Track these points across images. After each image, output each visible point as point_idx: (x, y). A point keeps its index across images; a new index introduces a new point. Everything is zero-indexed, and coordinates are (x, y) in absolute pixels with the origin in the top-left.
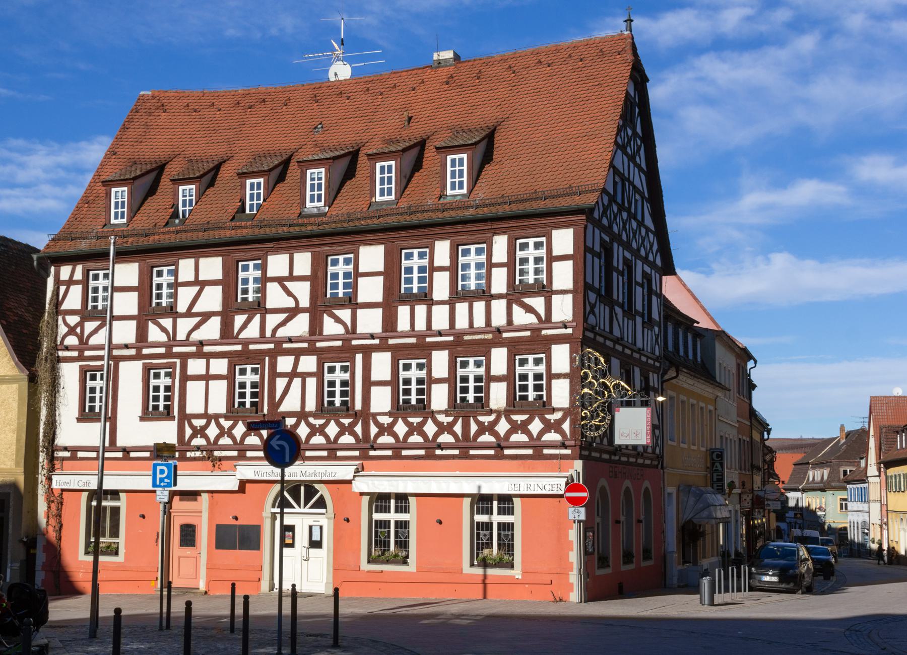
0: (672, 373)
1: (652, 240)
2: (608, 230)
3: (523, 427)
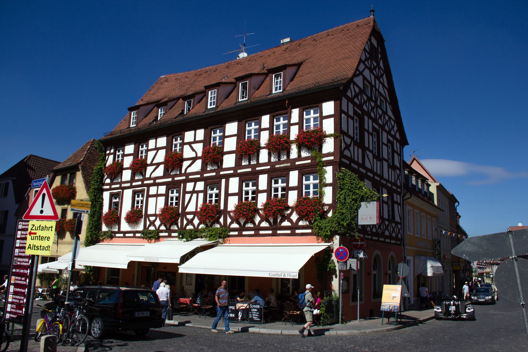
0: (408, 195)
1: (393, 124)
2: (360, 107)
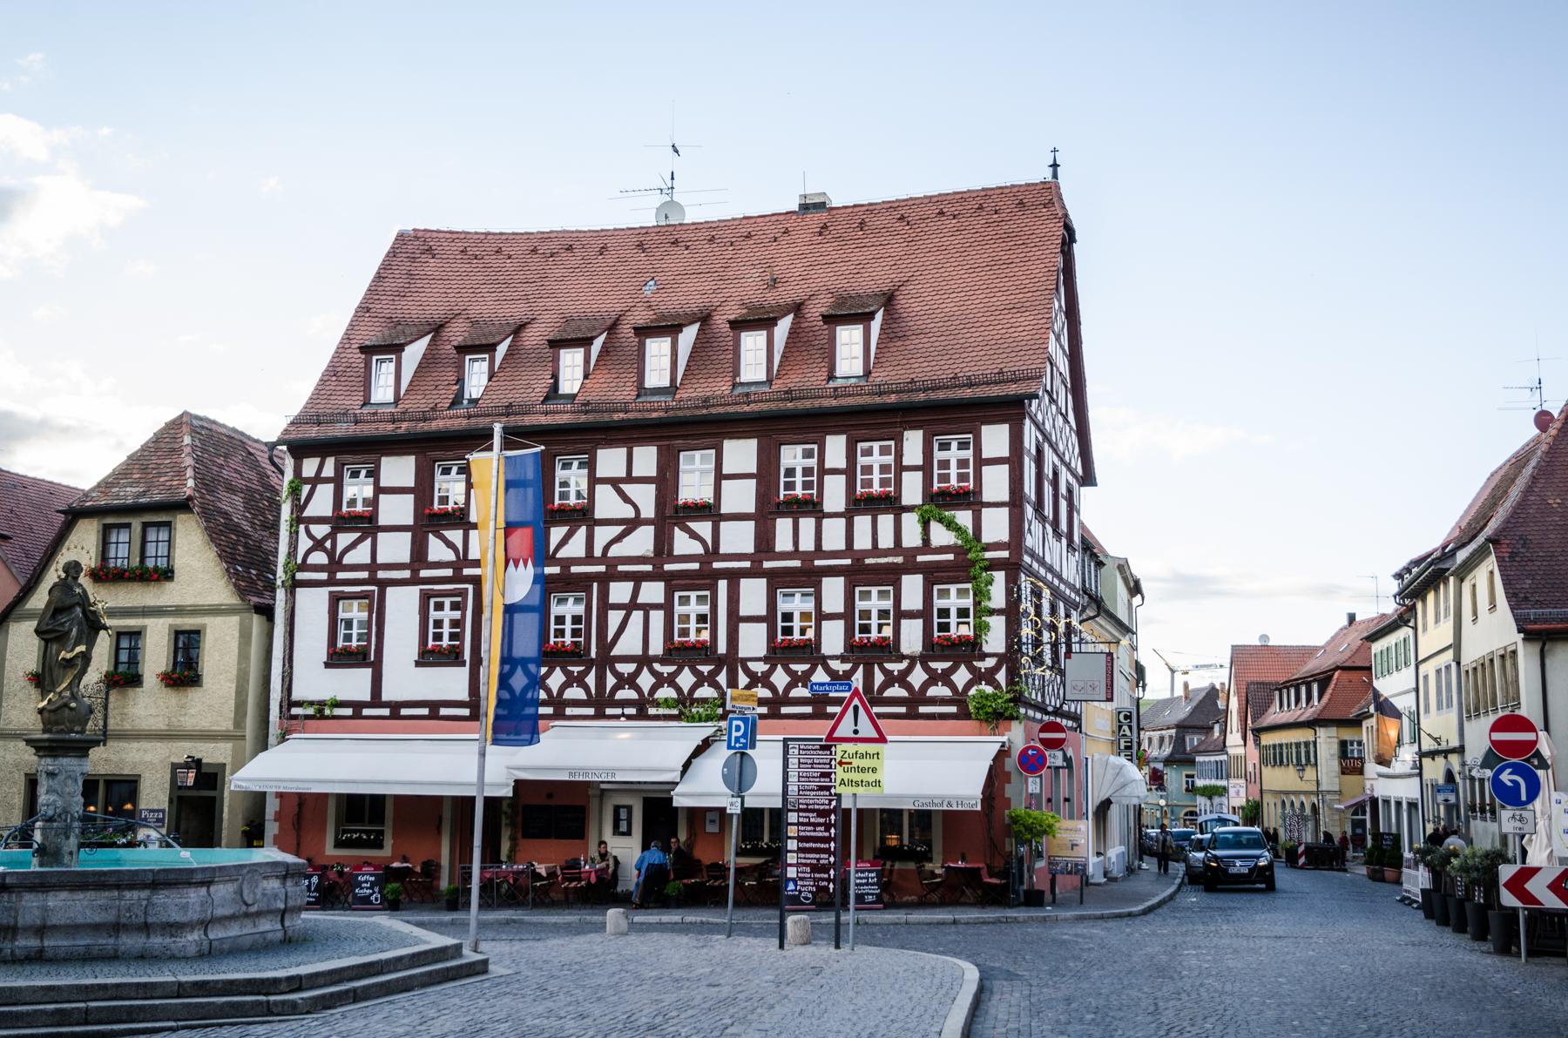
3: (945, 678)
